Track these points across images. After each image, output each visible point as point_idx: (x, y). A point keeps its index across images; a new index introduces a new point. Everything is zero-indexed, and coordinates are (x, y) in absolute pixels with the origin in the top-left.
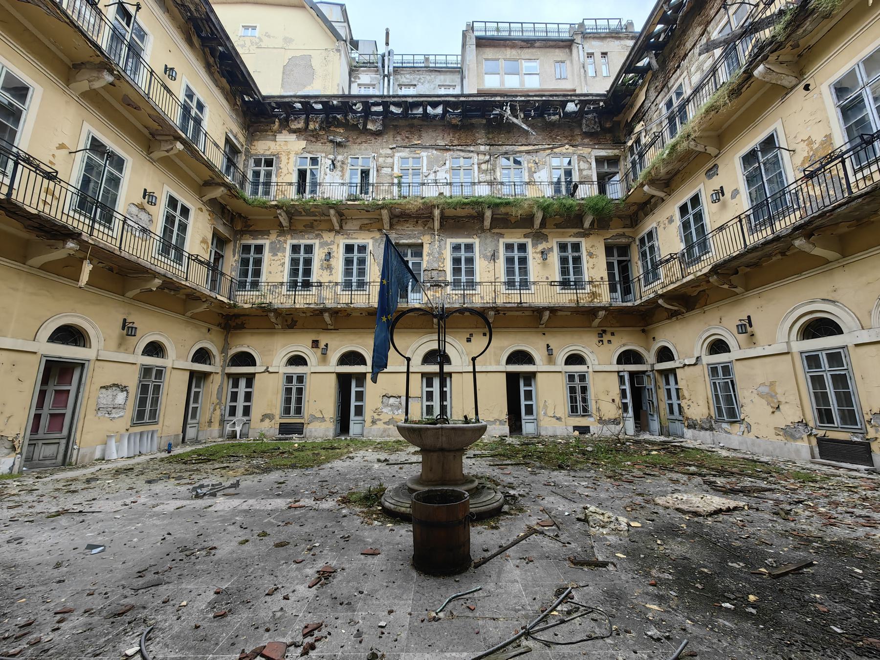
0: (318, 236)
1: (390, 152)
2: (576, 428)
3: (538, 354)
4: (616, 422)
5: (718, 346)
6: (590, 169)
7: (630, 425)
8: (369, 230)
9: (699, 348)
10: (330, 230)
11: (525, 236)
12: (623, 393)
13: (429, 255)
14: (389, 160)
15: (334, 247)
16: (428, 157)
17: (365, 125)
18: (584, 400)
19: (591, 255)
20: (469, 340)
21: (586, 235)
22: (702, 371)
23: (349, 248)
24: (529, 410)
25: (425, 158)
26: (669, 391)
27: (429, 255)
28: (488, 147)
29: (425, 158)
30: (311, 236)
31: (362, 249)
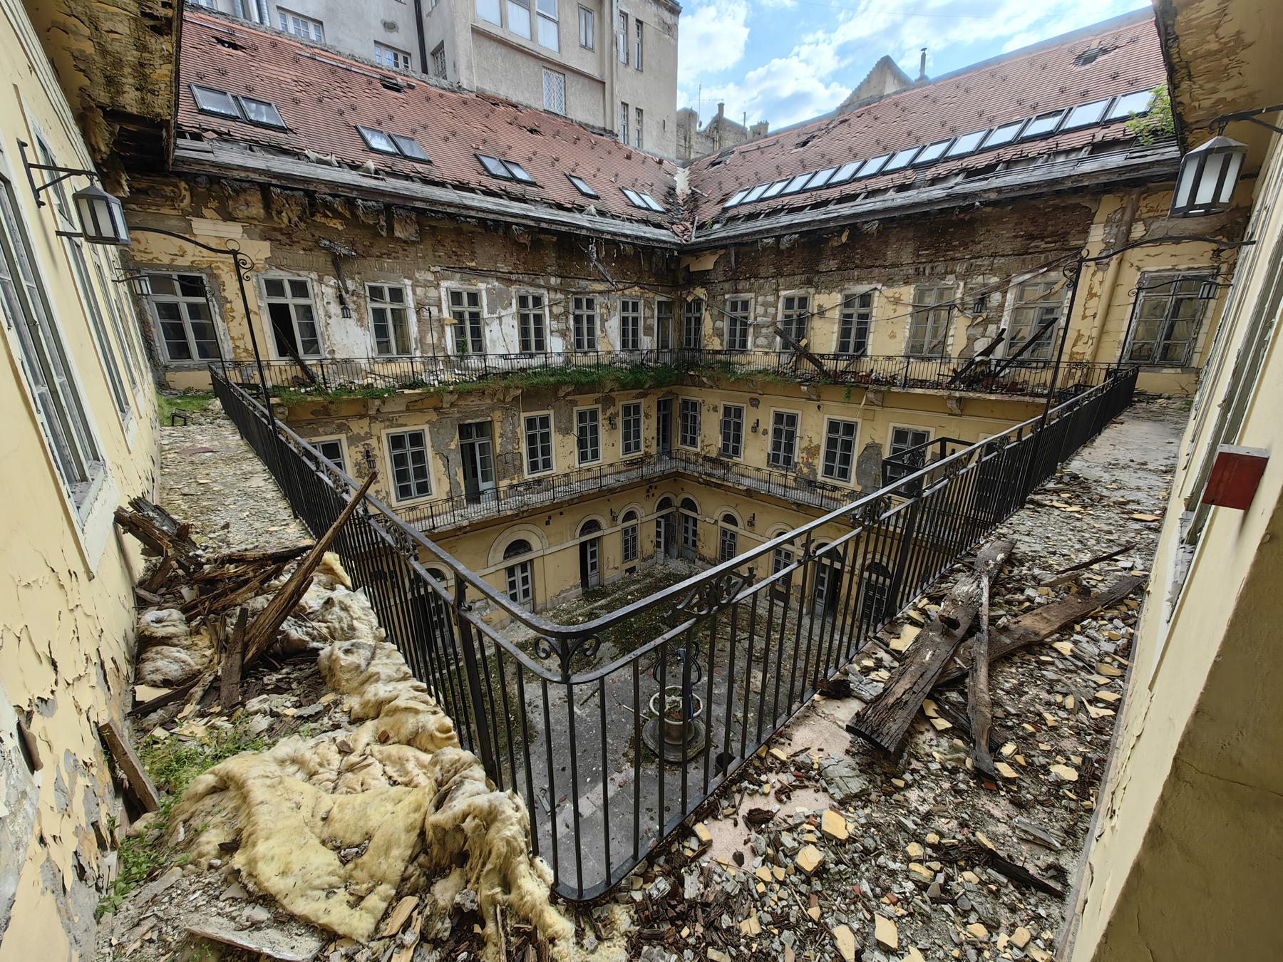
0: (342, 428)
1: (430, 277)
2: (627, 571)
3: (603, 522)
4: (652, 557)
5: (729, 519)
6: (653, 317)
7: (661, 555)
8: (421, 410)
9: (718, 515)
10: (362, 416)
11: (597, 402)
12: (658, 535)
13: (502, 436)
14: (432, 293)
15: (373, 442)
16: (487, 290)
17: (391, 229)
18: (634, 547)
19: (647, 416)
20: (548, 523)
21: (644, 395)
22: (716, 532)
23: (396, 441)
24: (594, 566)
25: (484, 294)
26: (686, 529)
27: (502, 436)
28: (559, 280)
29: (484, 294)
30: (329, 429)
31: (417, 439)
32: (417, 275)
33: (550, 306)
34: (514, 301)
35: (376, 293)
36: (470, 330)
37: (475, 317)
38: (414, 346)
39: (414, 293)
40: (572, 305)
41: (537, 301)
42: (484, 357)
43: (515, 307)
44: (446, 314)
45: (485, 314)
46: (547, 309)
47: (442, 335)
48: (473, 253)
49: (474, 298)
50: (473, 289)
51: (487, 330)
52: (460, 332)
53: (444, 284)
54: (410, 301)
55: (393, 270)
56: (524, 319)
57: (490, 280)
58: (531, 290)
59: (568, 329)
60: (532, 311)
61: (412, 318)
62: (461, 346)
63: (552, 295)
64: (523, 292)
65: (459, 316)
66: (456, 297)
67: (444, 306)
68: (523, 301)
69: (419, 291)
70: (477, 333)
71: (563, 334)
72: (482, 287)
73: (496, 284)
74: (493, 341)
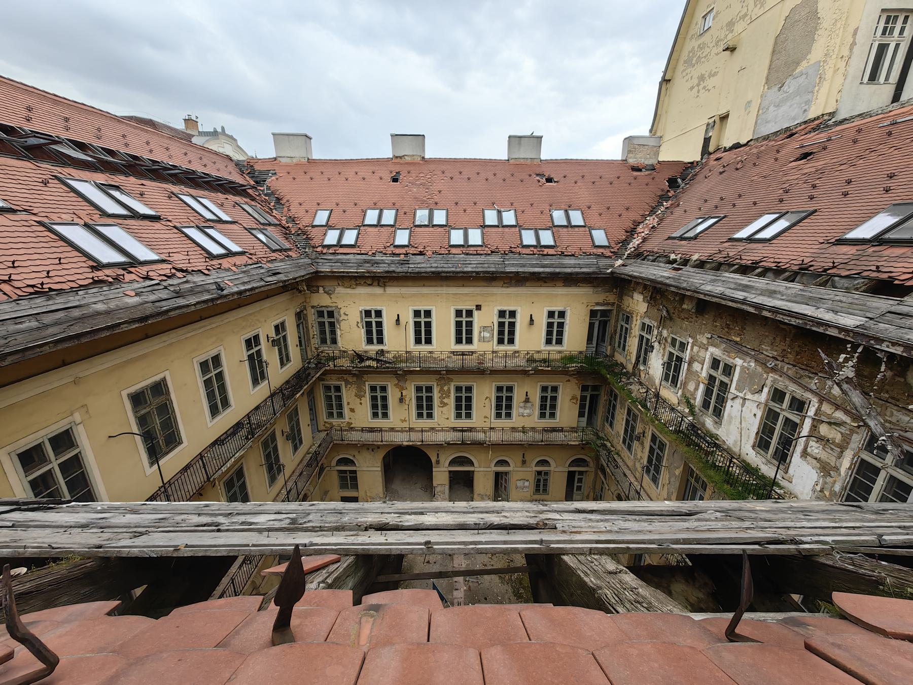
16: (742, 367)
25: (738, 370)
32: (698, 337)
33: (816, 423)
34: (766, 390)
35: (674, 341)
36: (717, 397)
37: (724, 387)
38: (679, 385)
39: (692, 350)
40: (858, 440)
41: (799, 405)
42: (718, 423)
43: (764, 396)
44: (704, 374)
45: (733, 389)
46: (808, 423)
47: (696, 389)
48: (743, 328)
49: (728, 370)
50: (730, 361)
51: (729, 403)
52: (708, 392)
53: (712, 349)
54: (687, 356)
55: (686, 330)
56: (771, 416)
57: (748, 359)
58: (792, 387)
59: (837, 469)
60: (785, 412)
61: (685, 366)
62: (706, 404)
63: (826, 408)
64: (780, 386)
65: (712, 378)
66: (715, 363)
67: (705, 367)
68: (778, 395)
69: (696, 349)
70: (721, 401)
71: (826, 469)
72: (739, 362)
73: (753, 364)
74: (730, 417)
